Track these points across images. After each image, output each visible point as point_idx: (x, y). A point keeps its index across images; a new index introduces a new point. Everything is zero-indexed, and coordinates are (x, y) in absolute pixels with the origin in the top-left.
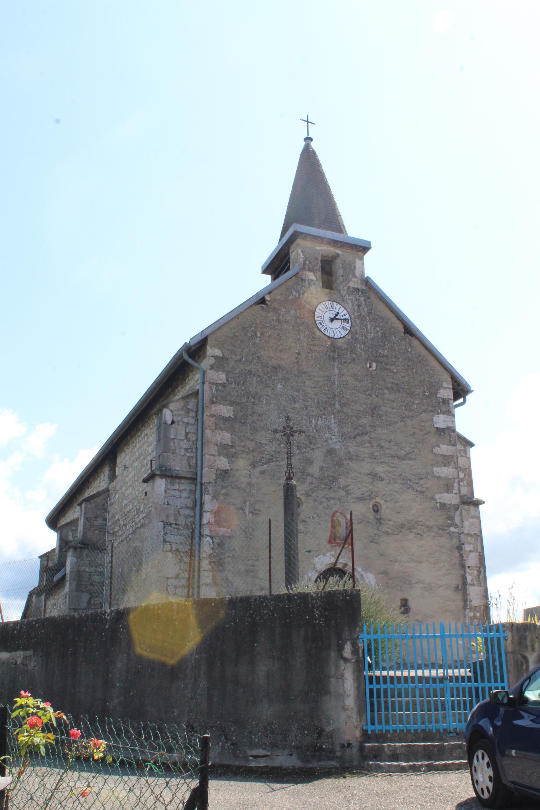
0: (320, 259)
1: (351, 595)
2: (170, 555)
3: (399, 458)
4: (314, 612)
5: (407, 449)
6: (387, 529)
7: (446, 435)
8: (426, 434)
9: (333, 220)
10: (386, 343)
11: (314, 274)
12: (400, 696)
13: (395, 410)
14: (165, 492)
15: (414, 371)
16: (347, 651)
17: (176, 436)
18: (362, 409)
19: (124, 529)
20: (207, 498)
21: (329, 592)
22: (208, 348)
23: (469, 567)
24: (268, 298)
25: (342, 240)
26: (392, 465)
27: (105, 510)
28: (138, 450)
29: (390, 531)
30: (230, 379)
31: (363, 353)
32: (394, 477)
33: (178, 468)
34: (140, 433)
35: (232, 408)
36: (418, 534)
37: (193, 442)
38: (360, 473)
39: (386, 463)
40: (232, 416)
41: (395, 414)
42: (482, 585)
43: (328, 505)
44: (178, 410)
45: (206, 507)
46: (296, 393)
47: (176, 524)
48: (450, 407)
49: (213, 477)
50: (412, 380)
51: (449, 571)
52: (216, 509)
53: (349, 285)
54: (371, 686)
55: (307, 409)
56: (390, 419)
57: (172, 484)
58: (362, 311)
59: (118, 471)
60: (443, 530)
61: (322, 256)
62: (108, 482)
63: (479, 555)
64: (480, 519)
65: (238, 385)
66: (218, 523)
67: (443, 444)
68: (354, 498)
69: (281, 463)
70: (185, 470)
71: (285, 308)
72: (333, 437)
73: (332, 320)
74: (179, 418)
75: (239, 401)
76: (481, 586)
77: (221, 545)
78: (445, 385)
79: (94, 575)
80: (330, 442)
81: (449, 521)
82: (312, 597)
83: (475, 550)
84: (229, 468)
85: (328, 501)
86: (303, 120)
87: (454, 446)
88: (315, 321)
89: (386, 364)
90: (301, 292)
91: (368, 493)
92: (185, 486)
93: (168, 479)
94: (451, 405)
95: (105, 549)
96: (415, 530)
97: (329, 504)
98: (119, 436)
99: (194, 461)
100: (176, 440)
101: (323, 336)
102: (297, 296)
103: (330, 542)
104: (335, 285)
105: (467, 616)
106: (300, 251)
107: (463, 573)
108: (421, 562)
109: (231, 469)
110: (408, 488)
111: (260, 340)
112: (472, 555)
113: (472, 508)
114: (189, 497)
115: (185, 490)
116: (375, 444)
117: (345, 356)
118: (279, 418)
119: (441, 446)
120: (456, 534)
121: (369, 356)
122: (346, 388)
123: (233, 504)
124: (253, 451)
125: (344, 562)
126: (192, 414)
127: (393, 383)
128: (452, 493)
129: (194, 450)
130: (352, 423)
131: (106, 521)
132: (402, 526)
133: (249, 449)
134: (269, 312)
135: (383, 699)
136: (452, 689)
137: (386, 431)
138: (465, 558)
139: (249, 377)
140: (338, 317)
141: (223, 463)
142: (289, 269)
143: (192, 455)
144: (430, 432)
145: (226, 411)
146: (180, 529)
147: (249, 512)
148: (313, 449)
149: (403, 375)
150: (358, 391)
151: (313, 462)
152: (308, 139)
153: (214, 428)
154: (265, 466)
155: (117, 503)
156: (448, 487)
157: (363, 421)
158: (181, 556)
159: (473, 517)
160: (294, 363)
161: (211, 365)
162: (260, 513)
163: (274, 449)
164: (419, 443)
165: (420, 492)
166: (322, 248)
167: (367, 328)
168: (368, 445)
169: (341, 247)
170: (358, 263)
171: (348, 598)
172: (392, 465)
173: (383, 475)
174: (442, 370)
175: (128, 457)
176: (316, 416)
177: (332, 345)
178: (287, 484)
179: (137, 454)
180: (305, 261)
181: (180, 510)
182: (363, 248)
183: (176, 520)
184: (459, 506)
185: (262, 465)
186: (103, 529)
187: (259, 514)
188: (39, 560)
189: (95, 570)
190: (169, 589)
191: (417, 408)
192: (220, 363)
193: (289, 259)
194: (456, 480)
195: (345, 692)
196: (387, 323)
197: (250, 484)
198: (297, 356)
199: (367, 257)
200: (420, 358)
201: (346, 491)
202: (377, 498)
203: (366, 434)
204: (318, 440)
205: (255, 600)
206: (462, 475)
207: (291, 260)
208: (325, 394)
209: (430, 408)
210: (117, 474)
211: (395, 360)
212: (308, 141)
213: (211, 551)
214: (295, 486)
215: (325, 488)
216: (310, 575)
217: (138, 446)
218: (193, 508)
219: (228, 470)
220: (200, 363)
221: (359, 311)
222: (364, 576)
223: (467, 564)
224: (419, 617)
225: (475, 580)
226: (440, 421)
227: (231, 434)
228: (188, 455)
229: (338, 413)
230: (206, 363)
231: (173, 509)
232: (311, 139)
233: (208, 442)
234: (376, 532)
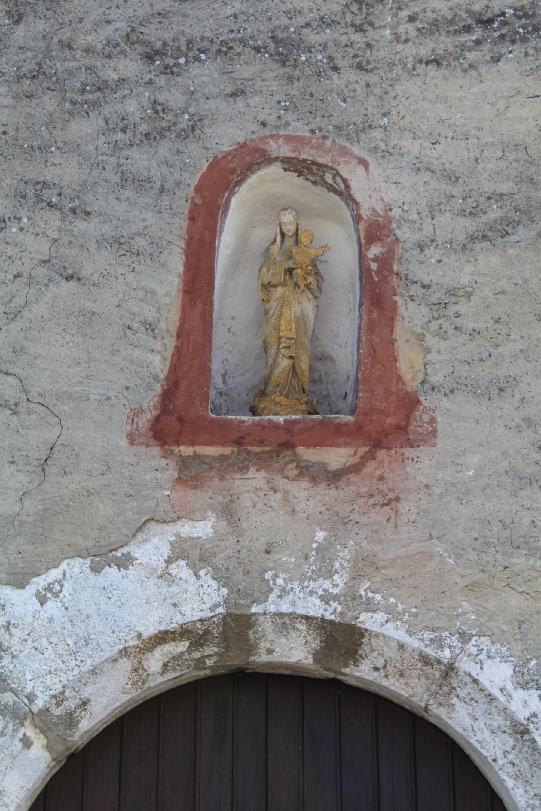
43: (158, 108)
97: (174, 98)
125: (314, 608)
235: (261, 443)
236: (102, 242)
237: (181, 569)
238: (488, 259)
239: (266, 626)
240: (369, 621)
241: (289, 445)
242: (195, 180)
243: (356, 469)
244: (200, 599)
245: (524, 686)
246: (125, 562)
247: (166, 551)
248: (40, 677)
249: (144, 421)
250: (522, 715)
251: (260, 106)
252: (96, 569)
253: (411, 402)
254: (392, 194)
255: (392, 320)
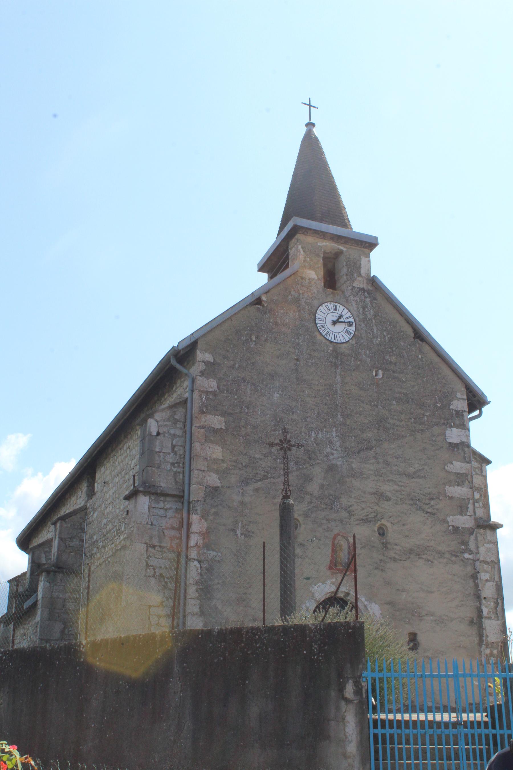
0: (322, 256)
1: (354, 628)
2: (153, 581)
3: (408, 475)
4: (313, 646)
5: (416, 466)
6: (394, 555)
7: (460, 451)
8: (438, 449)
9: (336, 214)
10: (394, 348)
11: (315, 272)
12: (408, 742)
13: (403, 423)
14: (149, 511)
15: (425, 379)
16: (349, 690)
17: (162, 449)
18: (366, 421)
19: (103, 551)
20: (195, 518)
21: (330, 623)
22: (198, 352)
23: (485, 598)
24: (264, 298)
25: (346, 236)
26: (400, 484)
27: (82, 530)
28: (119, 464)
29: (397, 557)
30: (221, 387)
31: (369, 360)
32: (402, 497)
33: (162, 485)
34: (121, 445)
35: (223, 419)
36: (429, 560)
37: (180, 455)
38: (365, 493)
39: (393, 481)
40: (224, 428)
41: (403, 427)
42: (500, 618)
44: (164, 420)
45: (195, 528)
46: (294, 403)
47: (160, 547)
48: (464, 420)
49: (202, 494)
50: (422, 390)
51: (462, 603)
52: (205, 530)
53: (354, 285)
54: (376, 731)
55: (306, 421)
56: (398, 433)
57: (157, 502)
58: (367, 313)
59: (97, 487)
60: (456, 556)
61: (325, 253)
62: (86, 499)
63: (497, 585)
64: (497, 545)
65: (230, 394)
66: (207, 546)
67: (456, 460)
68: (357, 520)
69: (277, 480)
70: (170, 486)
71: (283, 309)
72: (335, 452)
73: (334, 323)
74: (165, 429)
75: (232, 412)
76: (498, 620)
77: (209, 570)
78: (459, 395)
79: (69, 602)
80: (331, 457)
81: (463, 547)
82: (310, 629)
83: (492, 579)
84: (219, 485)
85: (329, 522)
86: (304, 104)
87: (468, 463)
88: (316, 324)
89: (394, 372)
90: (301, 292)
91: (374, 514)
92: (170, 504)
93: (151, 496)
94: (465, 418)
95: (81, 574)
96: (424, 557)
98: (98, 449)
99: (181, 477)
100: (161, 454)
101: (324, 340)
102: (296, 296)
103: (330, 568)
104: (338, 285)
105: (483, 653)
106: (300, 247)
107: (478, 604)
108: (431, 592)
109: (222, 487)
110: (417, 510)
111: (255, 344)
112: (489, 584)
113: (488, 532)
114: (175, 517)
115: (170, 508)
116: (381, 460)
117: (348, 363)
118: (275, 430)
119: (454, 462)
120: (471, 562)
121: (375, 363)
122: (349, 398)
123: (224, 525)
124: (246, 466)
125: (346, 591)
126: (180, 425)
127: (401, 393)
128: (466, 515)
129: (181, 465)
130: (355, 437)
131: (83, 542)
132: (411, 551)
133: (242, 464)
134: (265, 313)
135: (388, 746)
136: (466, 735)
137: (393, 446)
138: (480, 588)
139: (242, 385)
140: (341, 320)
141: (213, 479)
142: (287, 266)
143: (179, 470)
144: (442, 447)
145: (216, 421)
146: (165, 552)
147: (242, 534)
148: (312, 465)
149: (413, 384)
150: (363, 402)
151: (312, 480)
152: (310, 125)
153: (204, 441)
154: (260, 483)
155: (96, 522)
156: (462, 509)
157: (368, 434)
158: (166, 582)
159: (490, 542)
160: (293, 370)
161: (201, 372)
162: (253, 535)
163: (269, 465)
164: (429, 459)
165: (431, 513)
166: (325, 244)
167: (373, 332)
168: (373, 461)
169: (345, 243)
170: (363, 260)
171: (350, 631)
172: (400, 484)
173: (389, 495)
174: (456, 379)
175: (108, 472)
176: (316, 428)
177: (335, 350)
178: (284, 503)
179: (119, 468)
180: (305, 258)
181: (165, 531)
182: (369, 244)
183: (160, 541)
184: (474, 530)
185: (256, 482)
186: (79, 552)
188: (8, 584)
189: (69, 597)
190: (151, 619)
191: (427, 421)
192: (211, 369)
193: (288, 256)
194: (471, 501)
195: (346, 738)
196: (395, 327)
197: (242, 503)
198: (295, 362)
199: (374, 254)
200: (431, 366)
201: (348, 512)
202: (383, 520)
203: (371, 449)
204: (319, 455)
205: (247, 632)
206: (477, 496)
207: (290, 257)
208: (326, 404)
209: (442, 421)
210: (95, 491)
211: (404, 368)
212: (310, 127)
213: (198, 577)
214: (293, 505)
215: (326, 508)
216: (308, 605)
217: (119, 460)
218: (180, 529)
219: (218, 487)
220: (188, 370)
221: (364, 313)
222: (368, 607)
223: (483, 595)
224: (429, 654)
225: (492, 613)
226: (453, 435)
227: (222, 448)
228: (175, 470)
229: (340, 425)
230: (196, 369)
231: (157, 530)
232: (313, 125)
233: (197, 456)
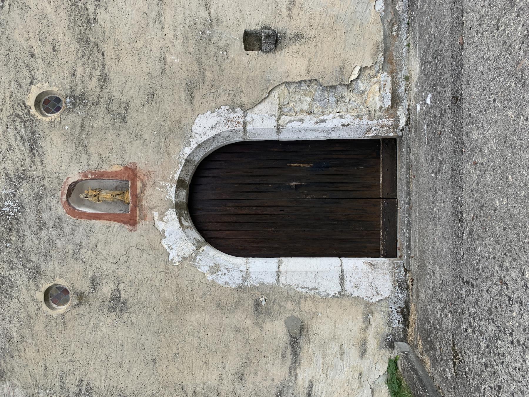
6: (95, 80)
29: (98, 73)
85: (44, 225)
96: (92, 9)
97: (51, 223)
125: (174, 190)
132: (84, 41)
162: (85, 383)
187: (88, 385)
202: (28, 104)
216: (205, 269)
234: (101, 109)
235: (136, 202)
236: (88, 239)
237: (165, 219)
238: (92, 150)
239: (178, 200)
240: (176, 177)
241: (136, 195)
242: (73, 218)
243: (142, 180)
244: (172, 214)
245: (190, 145)
246: (164, 231)
247: (161, 222)
248: (188, 248)
249: (131, 228)
250: (196, 145)
251: (54, 203)
252: (165, 237)
253: (126, 168)
254: (76, 172)
255: (106, 172)
